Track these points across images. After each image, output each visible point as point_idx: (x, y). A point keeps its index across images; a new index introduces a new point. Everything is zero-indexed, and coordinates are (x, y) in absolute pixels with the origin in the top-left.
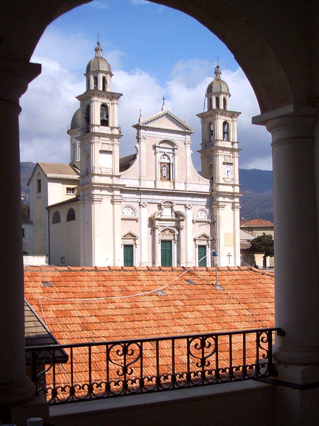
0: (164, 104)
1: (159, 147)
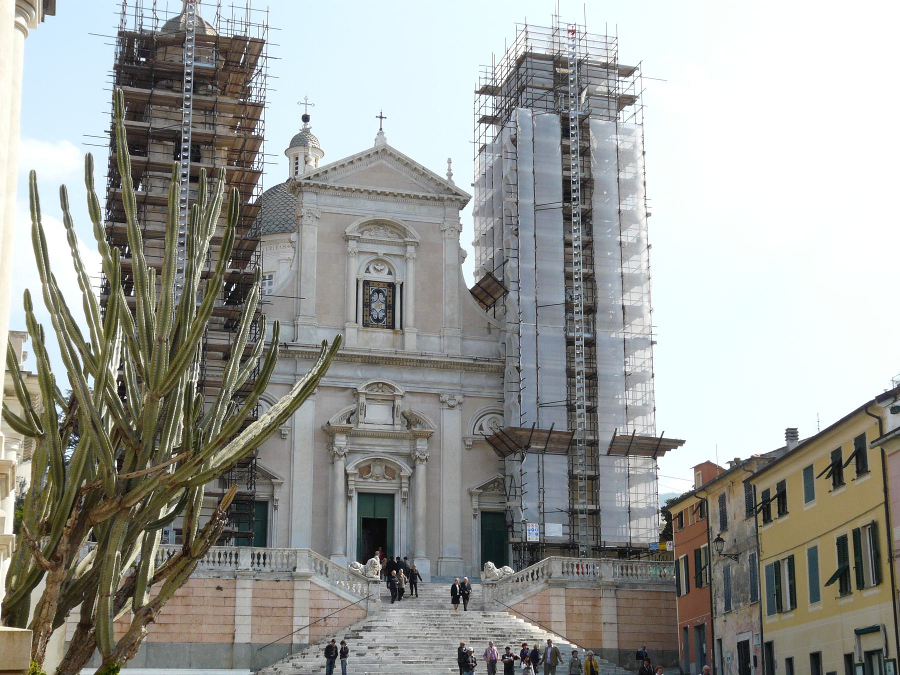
0: (381, 129)
1: (358, 240)
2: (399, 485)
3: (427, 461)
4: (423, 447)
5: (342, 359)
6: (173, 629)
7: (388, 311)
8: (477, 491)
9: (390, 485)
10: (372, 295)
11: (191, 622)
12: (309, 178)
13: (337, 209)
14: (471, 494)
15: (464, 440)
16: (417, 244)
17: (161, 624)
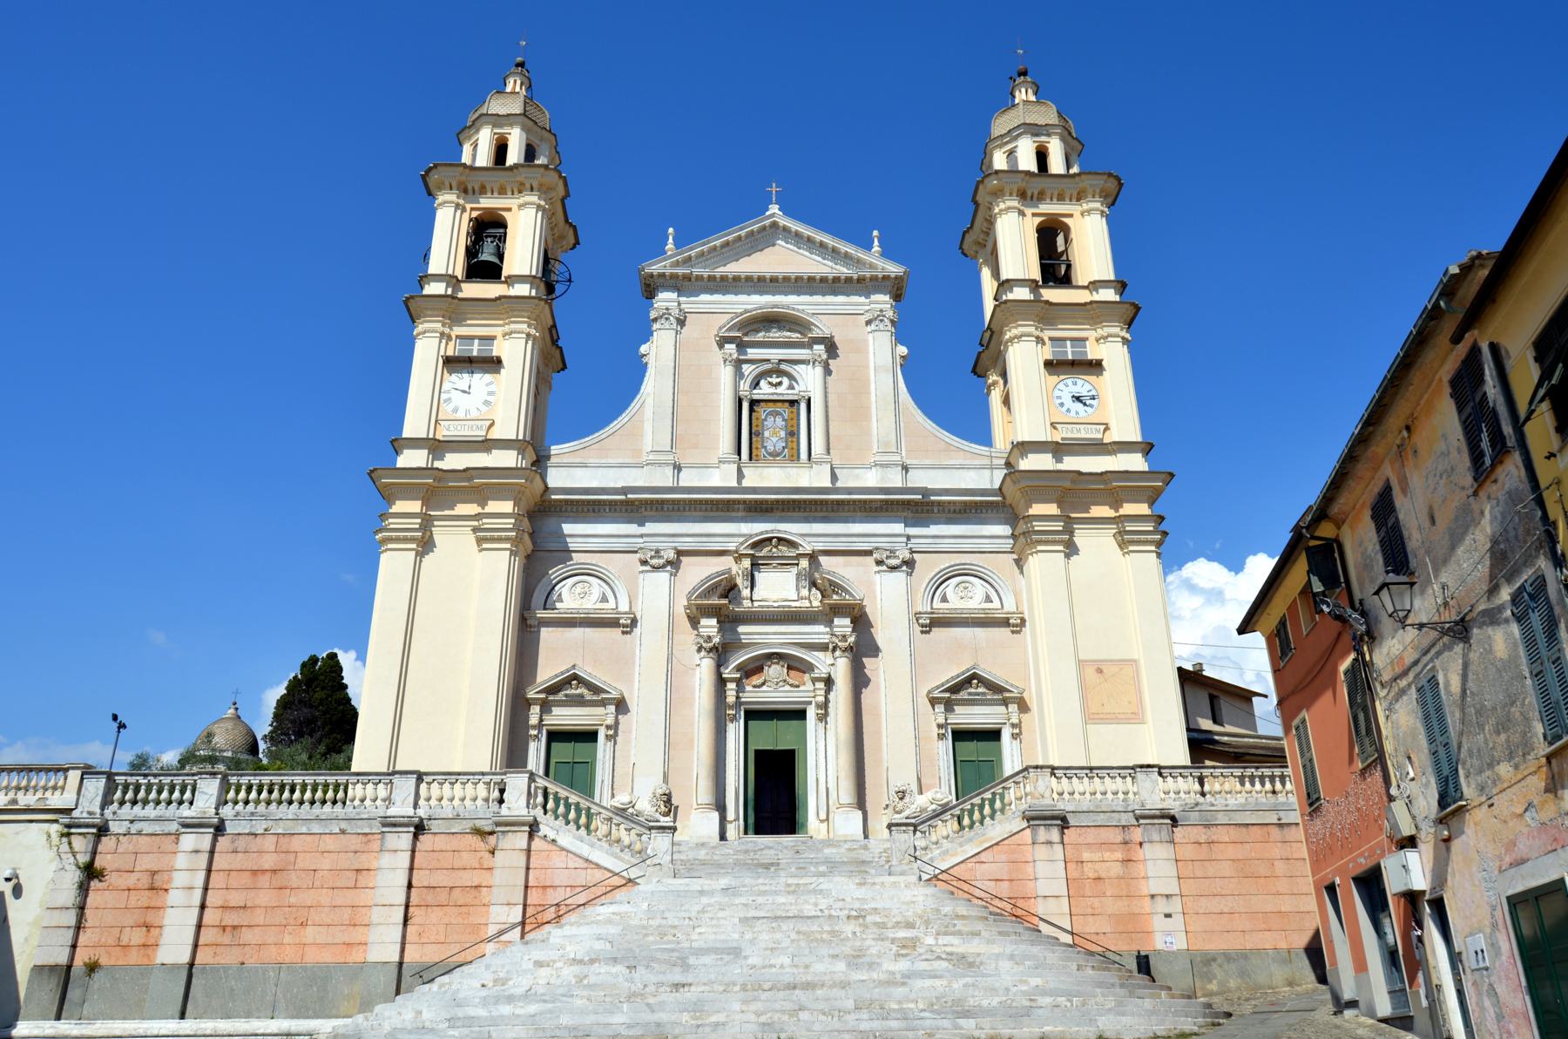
6: (247, 936)
10: (765, 420)
11: (284, 922)
15: (918, 616)
17: (224, 928)
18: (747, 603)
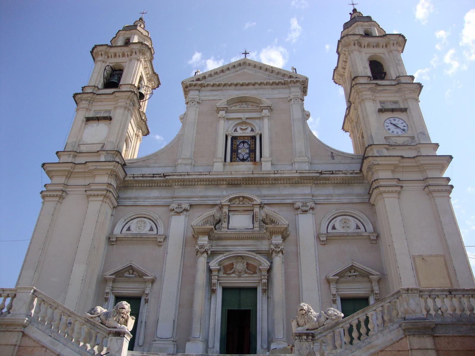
2: (259, 278)
3: (283, 253)
4: (278, 242)
5: (210, 183)
7: (251, 153)
8: (333, 278)
9: (251, 279)
12: (193, 81)
13: (213, 97)
14: (329, 281)
15: (318, 237)
16: (270, 108)
18: (224, 230)
